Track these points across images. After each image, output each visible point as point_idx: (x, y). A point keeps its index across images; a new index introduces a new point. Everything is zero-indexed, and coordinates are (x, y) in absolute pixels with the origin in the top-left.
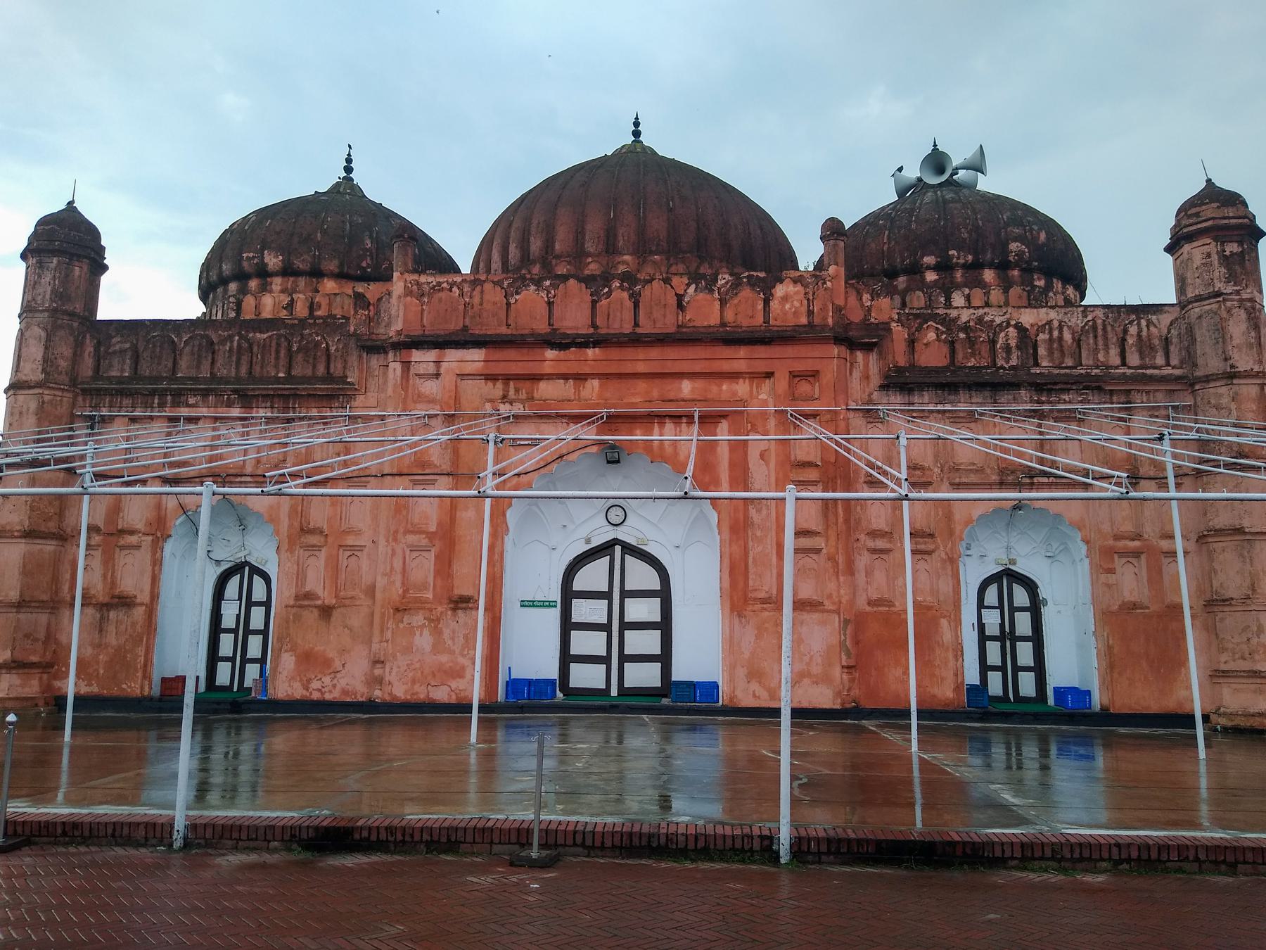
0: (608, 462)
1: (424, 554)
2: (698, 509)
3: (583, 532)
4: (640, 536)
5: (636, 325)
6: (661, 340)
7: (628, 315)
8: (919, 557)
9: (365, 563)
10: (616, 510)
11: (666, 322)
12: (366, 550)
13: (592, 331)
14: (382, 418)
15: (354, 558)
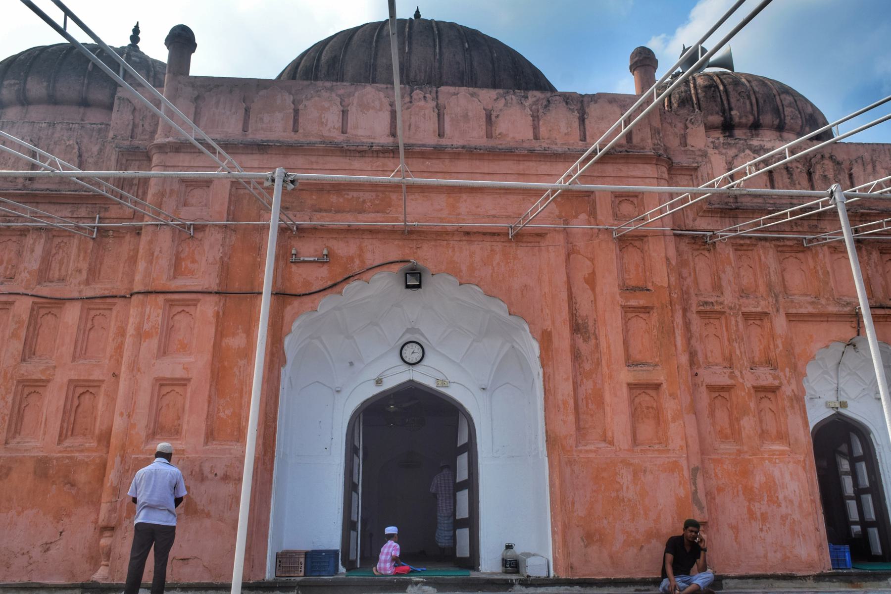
0: (408, 287)
1: (177, 389)
2: (507, 347)
3: (373, 373)
4: (441, 377)
5: (441, 135)
6: (471, 153)
7: (431, 125)
8: (762, 395)
9: (101, 402)
10: (412, 349)
11: (476, 136)
12: (104, 387)
13: (391, 139)
14: (138, 231)
15: (87, 396)
